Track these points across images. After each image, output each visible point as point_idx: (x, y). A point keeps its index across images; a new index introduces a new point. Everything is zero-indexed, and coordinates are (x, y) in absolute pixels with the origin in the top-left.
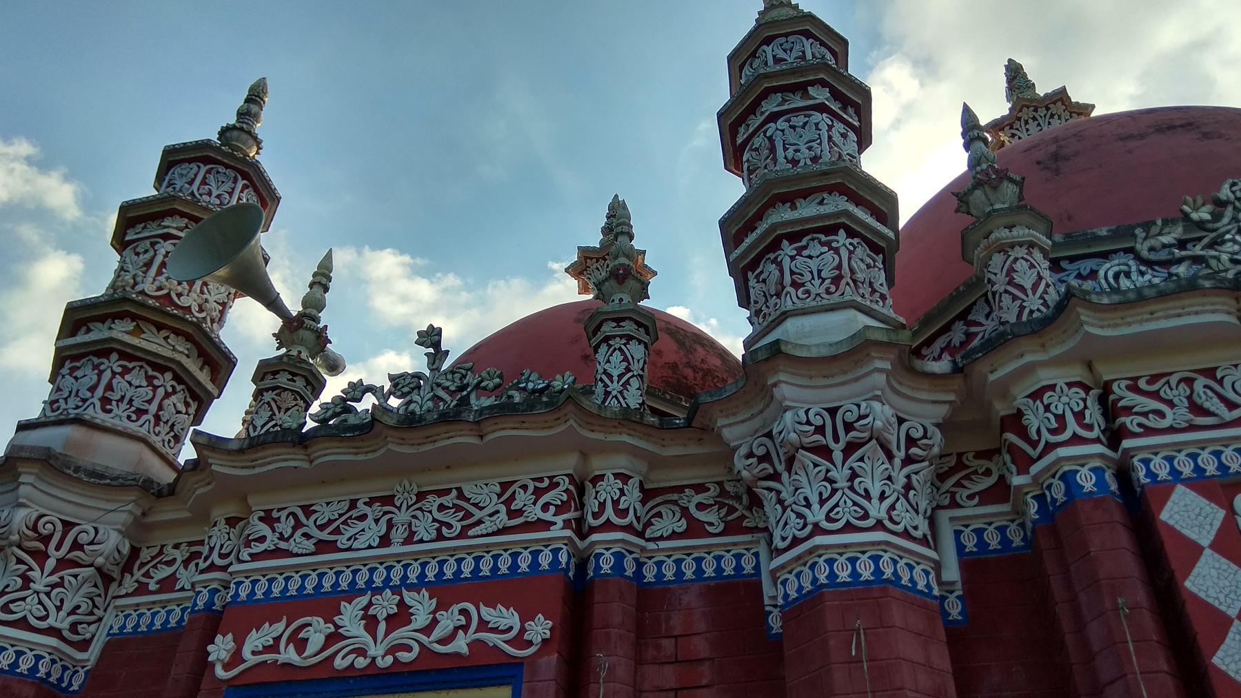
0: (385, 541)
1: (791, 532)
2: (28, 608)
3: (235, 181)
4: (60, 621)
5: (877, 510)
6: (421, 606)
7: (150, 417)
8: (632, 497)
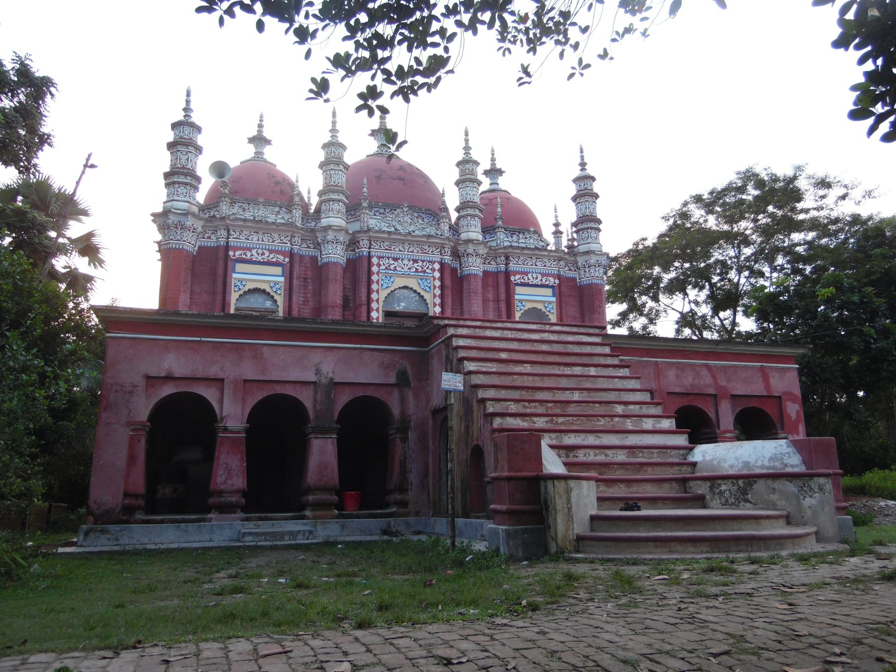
0: (258, 240)
1: (326, 252)
4: (193, 242)
5: (338, 252)
6: (267, 253)
8: (300, 241)
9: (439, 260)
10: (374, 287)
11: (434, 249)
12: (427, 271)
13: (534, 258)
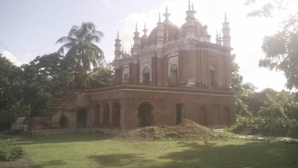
9: (151, 57)
10: (140, 68)
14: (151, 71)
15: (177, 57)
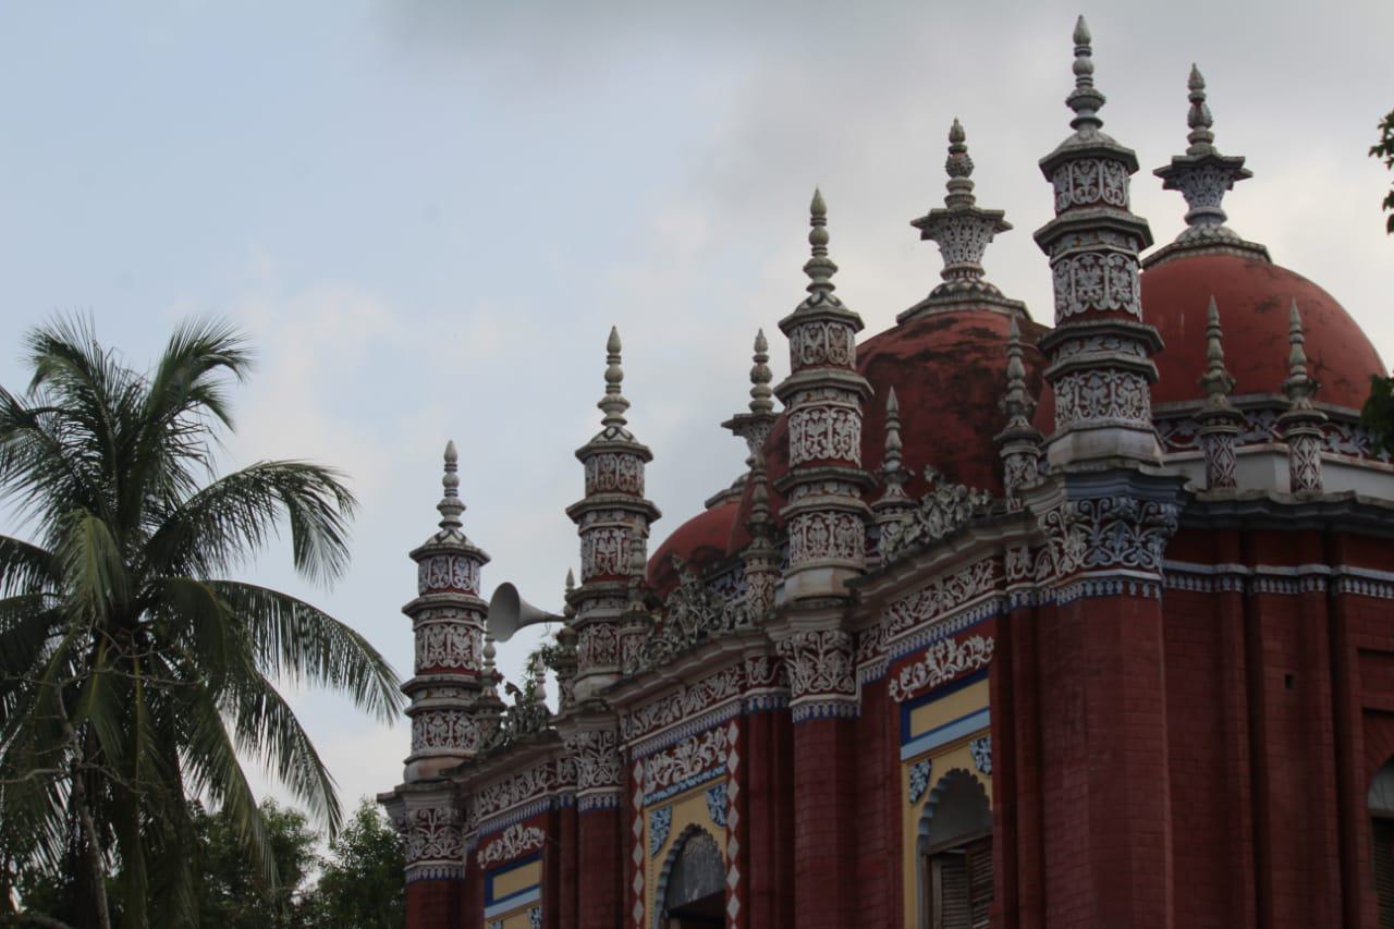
2: (432, 851)
3: (447, 562)
6: (519, 827)
7: (450, 740)
9: (734, 710)
11: (728, 677)
12: (722, 759)
13: (939, 585)
14: (734, 877)
15: (979, 695)
